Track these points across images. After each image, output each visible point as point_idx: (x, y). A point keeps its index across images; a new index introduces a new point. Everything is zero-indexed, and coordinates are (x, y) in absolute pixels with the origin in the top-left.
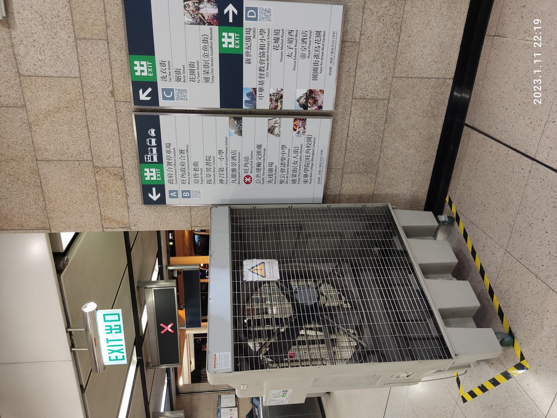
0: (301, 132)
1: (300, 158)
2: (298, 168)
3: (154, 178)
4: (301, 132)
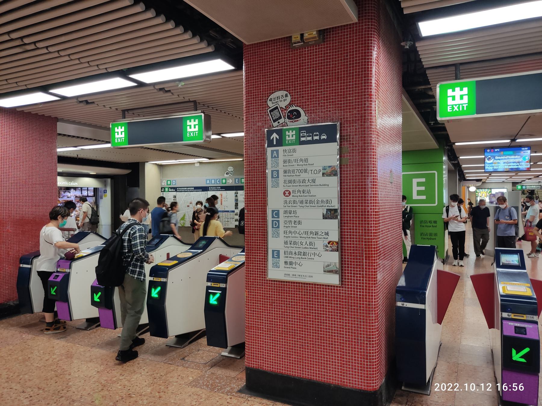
0: (328, 249)
1: (306, 248)
2: (297, 246)
3: (287, 138)
4: (328, 249)
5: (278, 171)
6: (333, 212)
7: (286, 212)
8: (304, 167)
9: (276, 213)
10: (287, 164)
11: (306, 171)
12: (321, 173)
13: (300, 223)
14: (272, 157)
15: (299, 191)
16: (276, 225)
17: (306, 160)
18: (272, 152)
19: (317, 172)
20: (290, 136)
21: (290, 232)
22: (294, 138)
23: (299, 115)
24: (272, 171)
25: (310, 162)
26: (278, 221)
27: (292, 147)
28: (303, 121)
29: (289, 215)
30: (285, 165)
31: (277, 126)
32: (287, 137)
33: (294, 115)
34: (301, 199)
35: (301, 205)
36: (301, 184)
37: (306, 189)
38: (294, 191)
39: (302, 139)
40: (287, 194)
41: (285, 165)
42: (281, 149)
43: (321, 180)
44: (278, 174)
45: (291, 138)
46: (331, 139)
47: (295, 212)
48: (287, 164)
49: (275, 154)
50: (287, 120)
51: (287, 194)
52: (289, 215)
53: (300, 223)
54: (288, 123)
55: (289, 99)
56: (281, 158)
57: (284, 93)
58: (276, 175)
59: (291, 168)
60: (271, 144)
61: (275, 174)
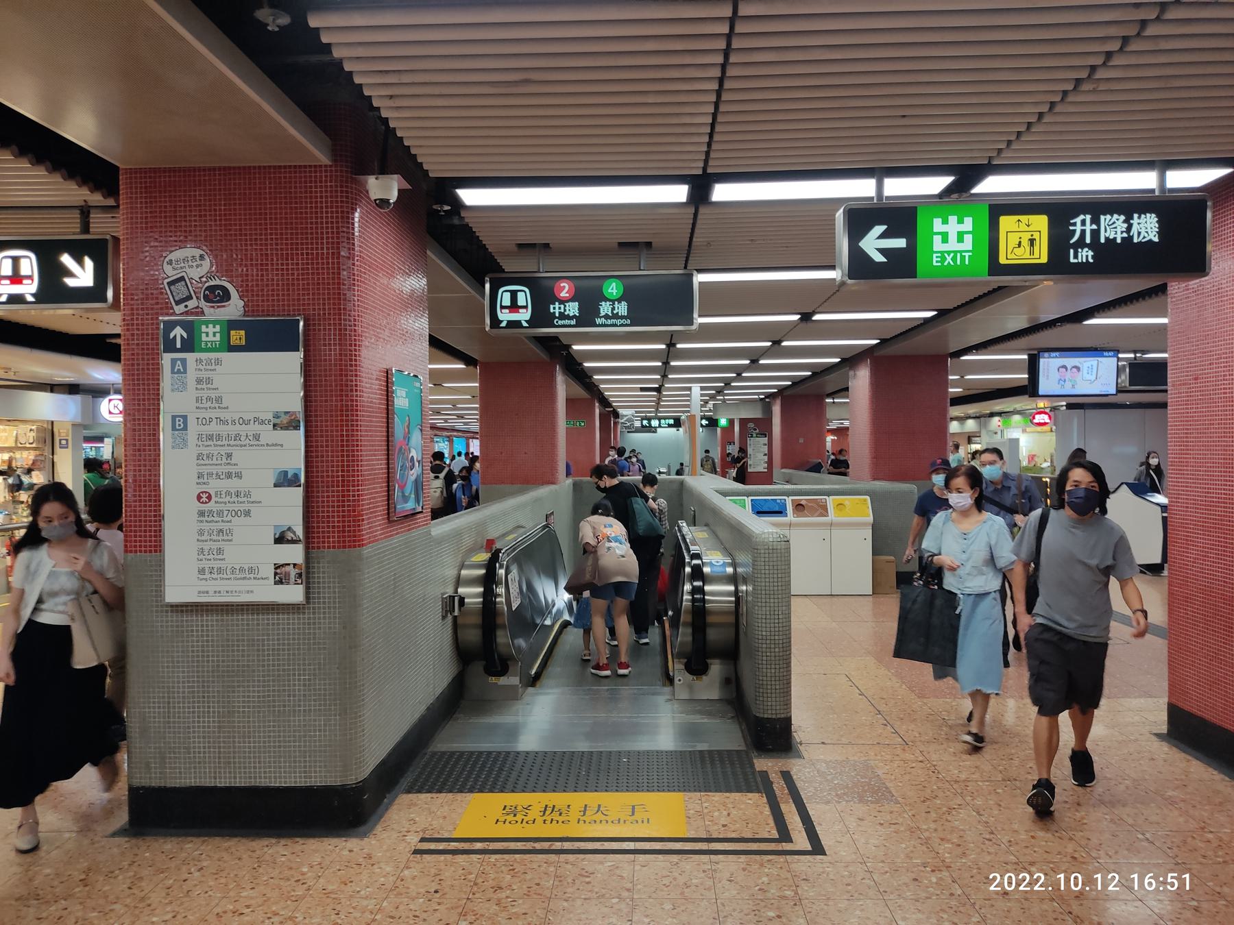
10: (204, 386)
14: (173, 372)
18: (174, 361)
20: (210, 334)
22: (218, 337)
23: (226, 296)
33: (217, 296)
45: (211, 338)
48: (204, 386)
49: (179, 366)
50: (203, 303)
54: (206, 310)
60: (170, 347)
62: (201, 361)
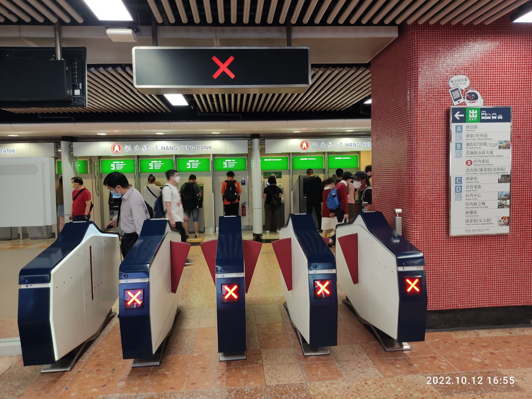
5: (461, 144)
6: (506, 177)
7: (467, 179)
8: (484, 141)
9: (459, 180)
10: (470, 138)
11: (485, 144)
12: (497, 147)
13: (479, 187)
14: (456, 132)
15: (479, 161)
16: (458, 189)
17: (486, 135)
18: (457, 127)
19: (494, 145)
20: (473, 114)
21: (471, 195)
22: (476, 116)
23: (476, 98)
24: (456, 144)
25: (489, 137)
26: (461, 187)
27: (474, 124)
28: (480, 103)
29: (470, 181)
30: (468, 138)
31: (458, 105)
32: (470, 115)
33: (473, 97)
34: (481, 167)
35: (481, 172)
36: (481, 155)
37: (485, 159)
38: (475, 161)
39: (483, 118)
40: (469, 164)
41: (468, 138)
42: (464, 125)
43: (497, 151)
44: (461, 146)
45: (473, 116)
46: (506, 119)
47: (476, 178)
48: (470, 138)
50: (466, 101)
51: (469, 164)
52: (470, 181)
53: (479, 187)
54: (467, 103)
55: (468, 83)
56: (464, 133)
57: (464, 77)
58: (460, 146)
59: (473, 142)
60: (455, 120)
61: (459, 146)
62: (469, 127)
